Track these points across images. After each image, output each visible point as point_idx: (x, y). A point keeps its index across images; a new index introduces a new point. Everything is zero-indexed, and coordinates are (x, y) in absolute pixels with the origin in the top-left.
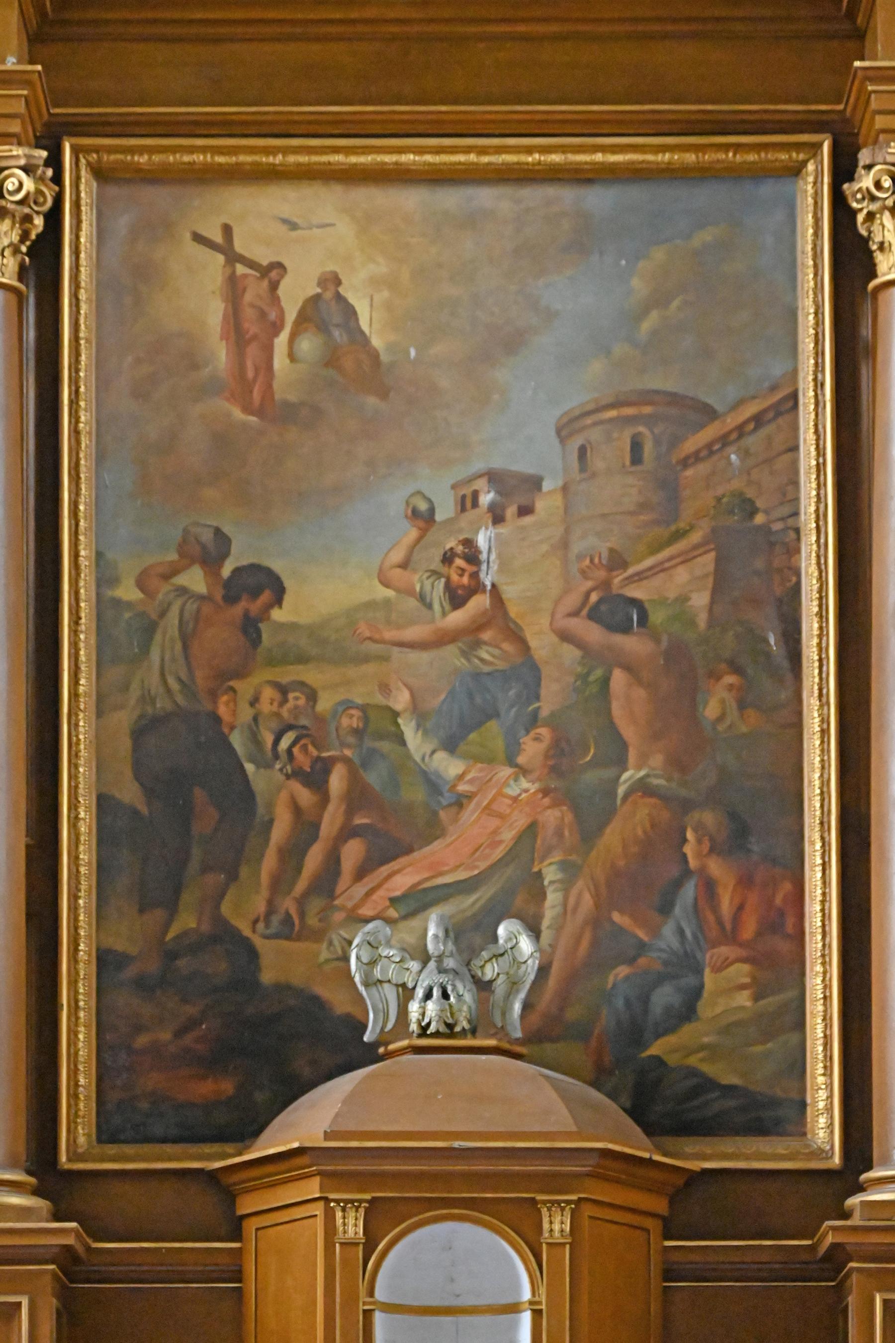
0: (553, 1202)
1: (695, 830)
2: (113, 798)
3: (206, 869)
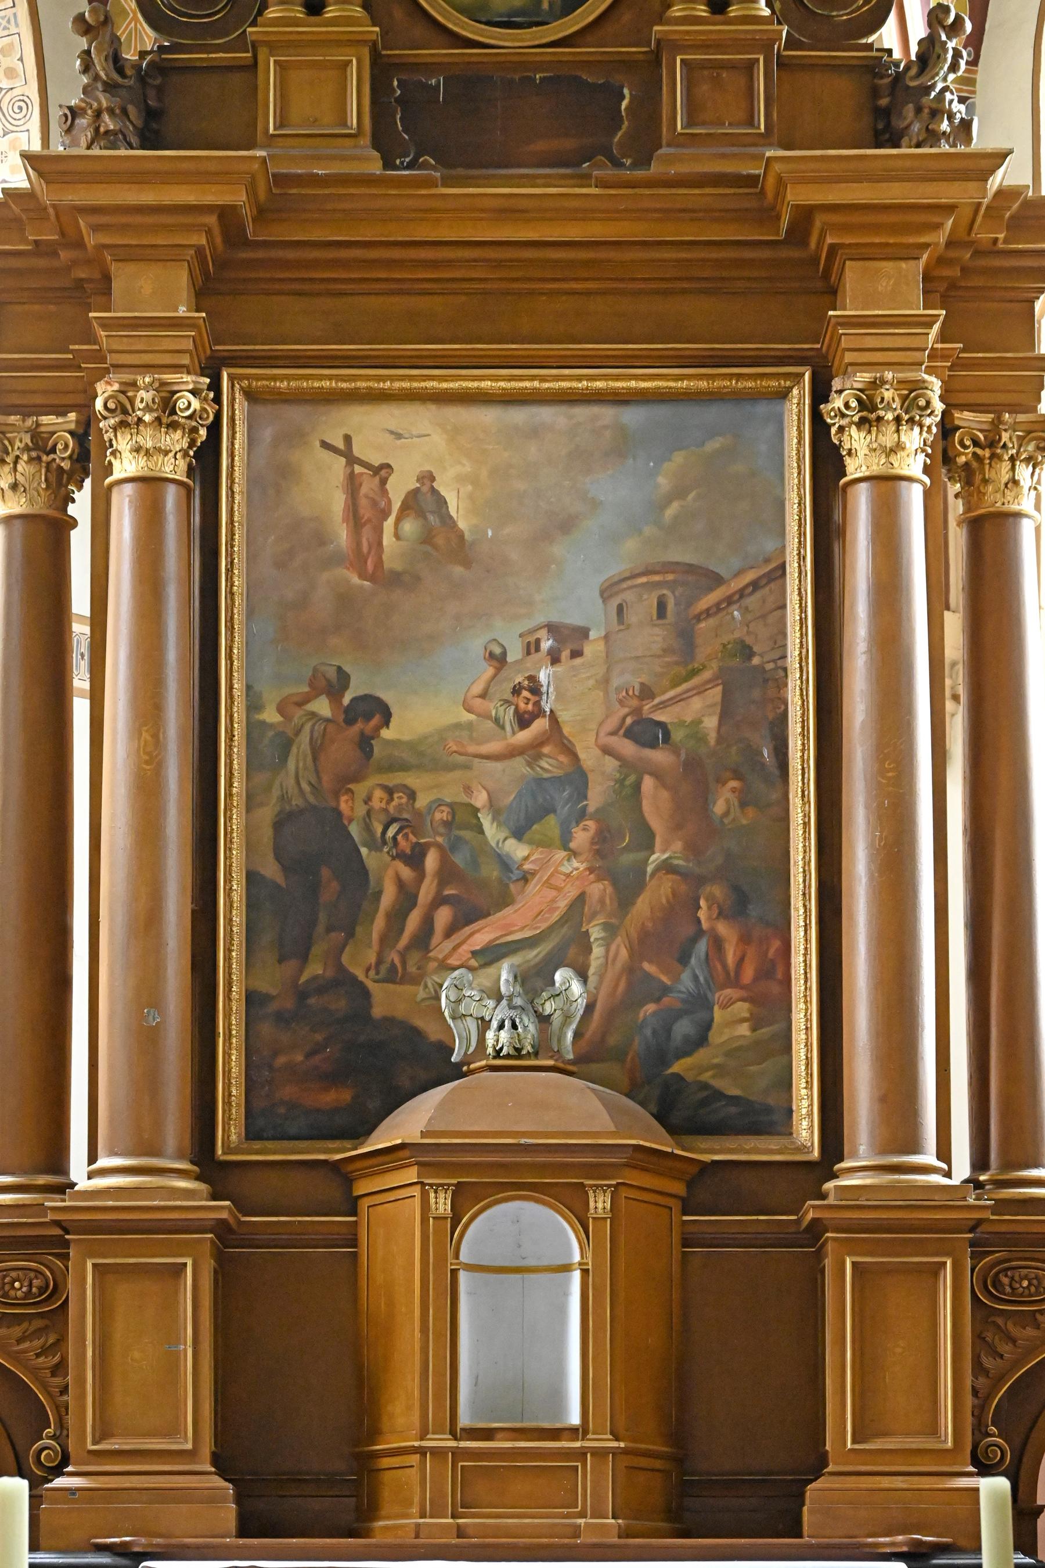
0: (597, 1186)
1: (707, 900)
2: (258, 873)
3: (329, 929)
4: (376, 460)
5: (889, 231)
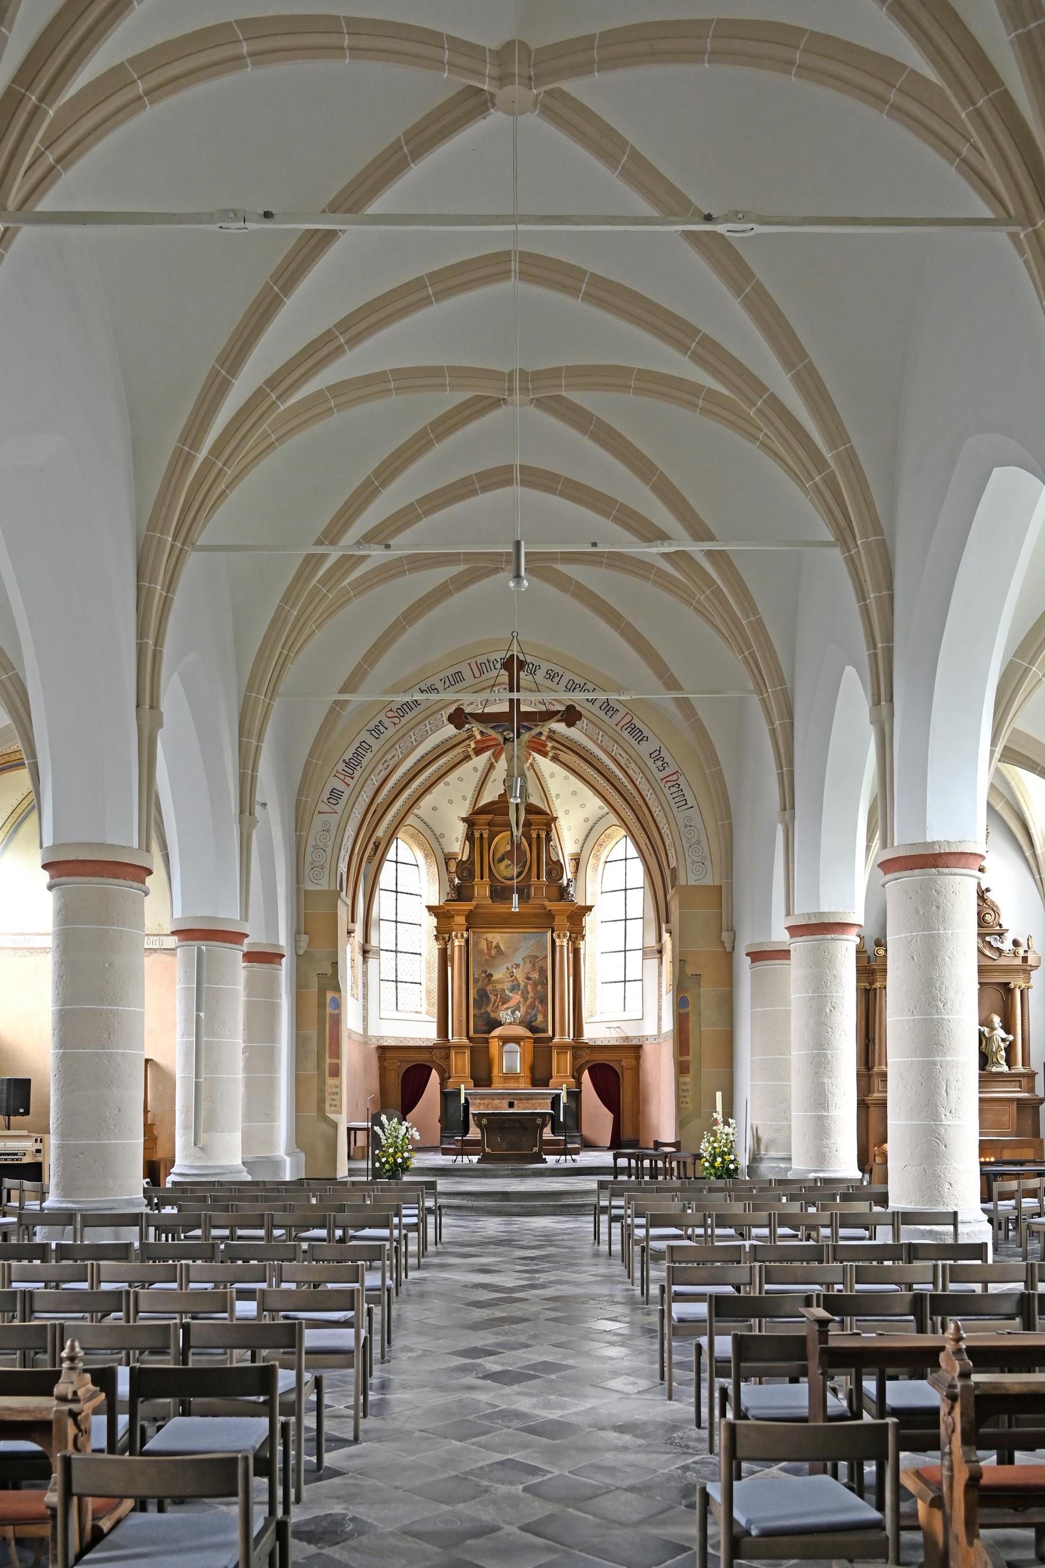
5: (562, 912)
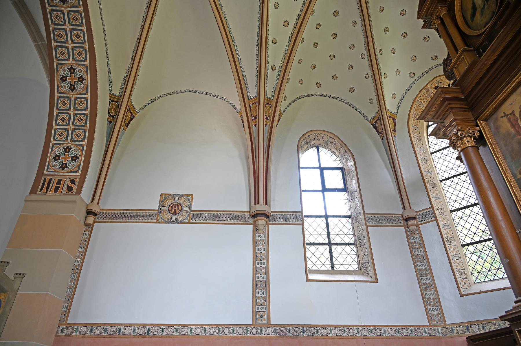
4: (510, 112)
